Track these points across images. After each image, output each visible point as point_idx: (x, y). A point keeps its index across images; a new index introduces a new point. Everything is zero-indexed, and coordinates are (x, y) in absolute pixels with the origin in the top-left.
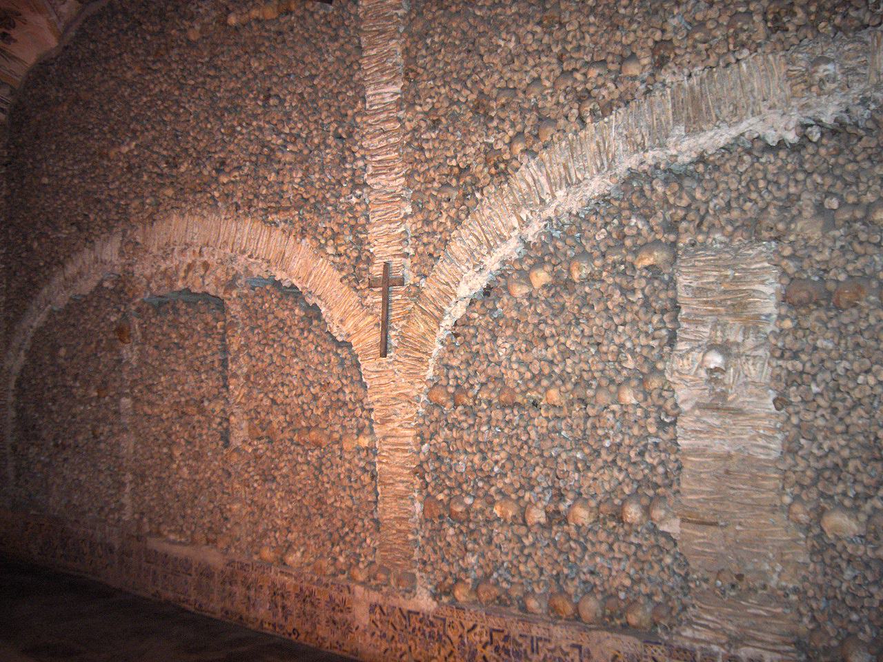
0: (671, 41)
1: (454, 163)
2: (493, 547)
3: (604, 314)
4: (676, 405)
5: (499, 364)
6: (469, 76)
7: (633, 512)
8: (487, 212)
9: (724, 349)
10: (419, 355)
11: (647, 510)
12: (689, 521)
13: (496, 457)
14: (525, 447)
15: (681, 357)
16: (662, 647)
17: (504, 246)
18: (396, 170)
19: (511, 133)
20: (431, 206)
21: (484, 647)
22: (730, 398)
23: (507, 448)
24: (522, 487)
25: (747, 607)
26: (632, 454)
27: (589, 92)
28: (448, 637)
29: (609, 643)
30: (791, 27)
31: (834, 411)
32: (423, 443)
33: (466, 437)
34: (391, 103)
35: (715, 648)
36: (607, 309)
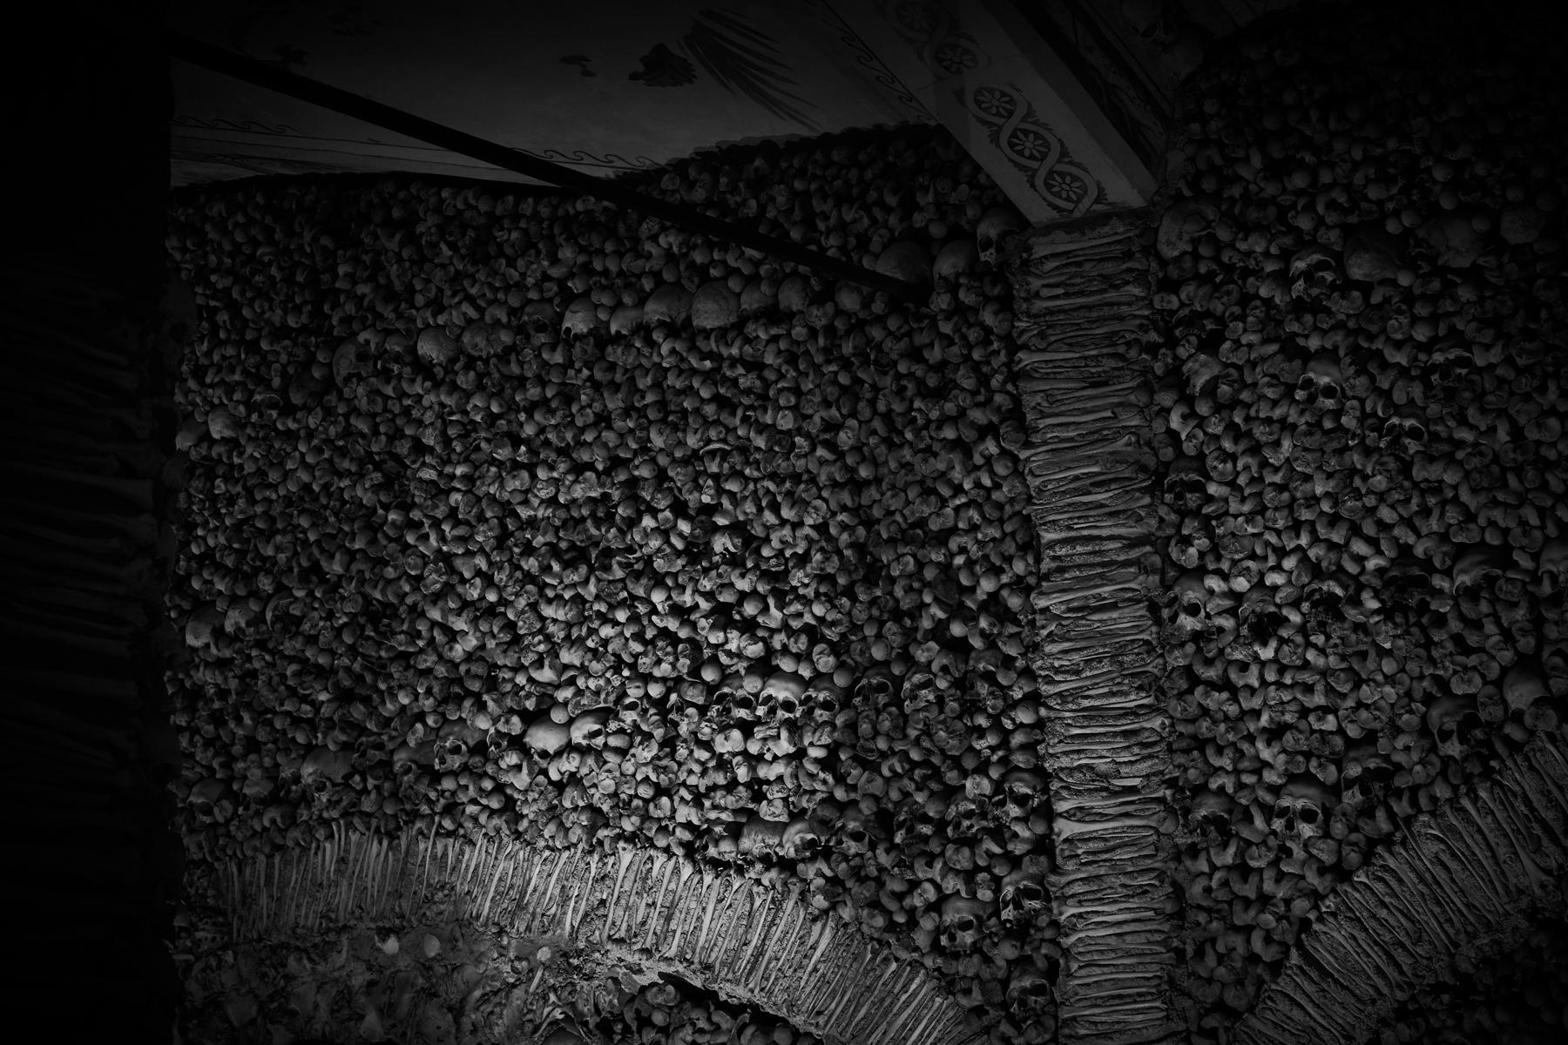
1: (1330, 723)
6: (1371, 511)
19: (1507, 656)
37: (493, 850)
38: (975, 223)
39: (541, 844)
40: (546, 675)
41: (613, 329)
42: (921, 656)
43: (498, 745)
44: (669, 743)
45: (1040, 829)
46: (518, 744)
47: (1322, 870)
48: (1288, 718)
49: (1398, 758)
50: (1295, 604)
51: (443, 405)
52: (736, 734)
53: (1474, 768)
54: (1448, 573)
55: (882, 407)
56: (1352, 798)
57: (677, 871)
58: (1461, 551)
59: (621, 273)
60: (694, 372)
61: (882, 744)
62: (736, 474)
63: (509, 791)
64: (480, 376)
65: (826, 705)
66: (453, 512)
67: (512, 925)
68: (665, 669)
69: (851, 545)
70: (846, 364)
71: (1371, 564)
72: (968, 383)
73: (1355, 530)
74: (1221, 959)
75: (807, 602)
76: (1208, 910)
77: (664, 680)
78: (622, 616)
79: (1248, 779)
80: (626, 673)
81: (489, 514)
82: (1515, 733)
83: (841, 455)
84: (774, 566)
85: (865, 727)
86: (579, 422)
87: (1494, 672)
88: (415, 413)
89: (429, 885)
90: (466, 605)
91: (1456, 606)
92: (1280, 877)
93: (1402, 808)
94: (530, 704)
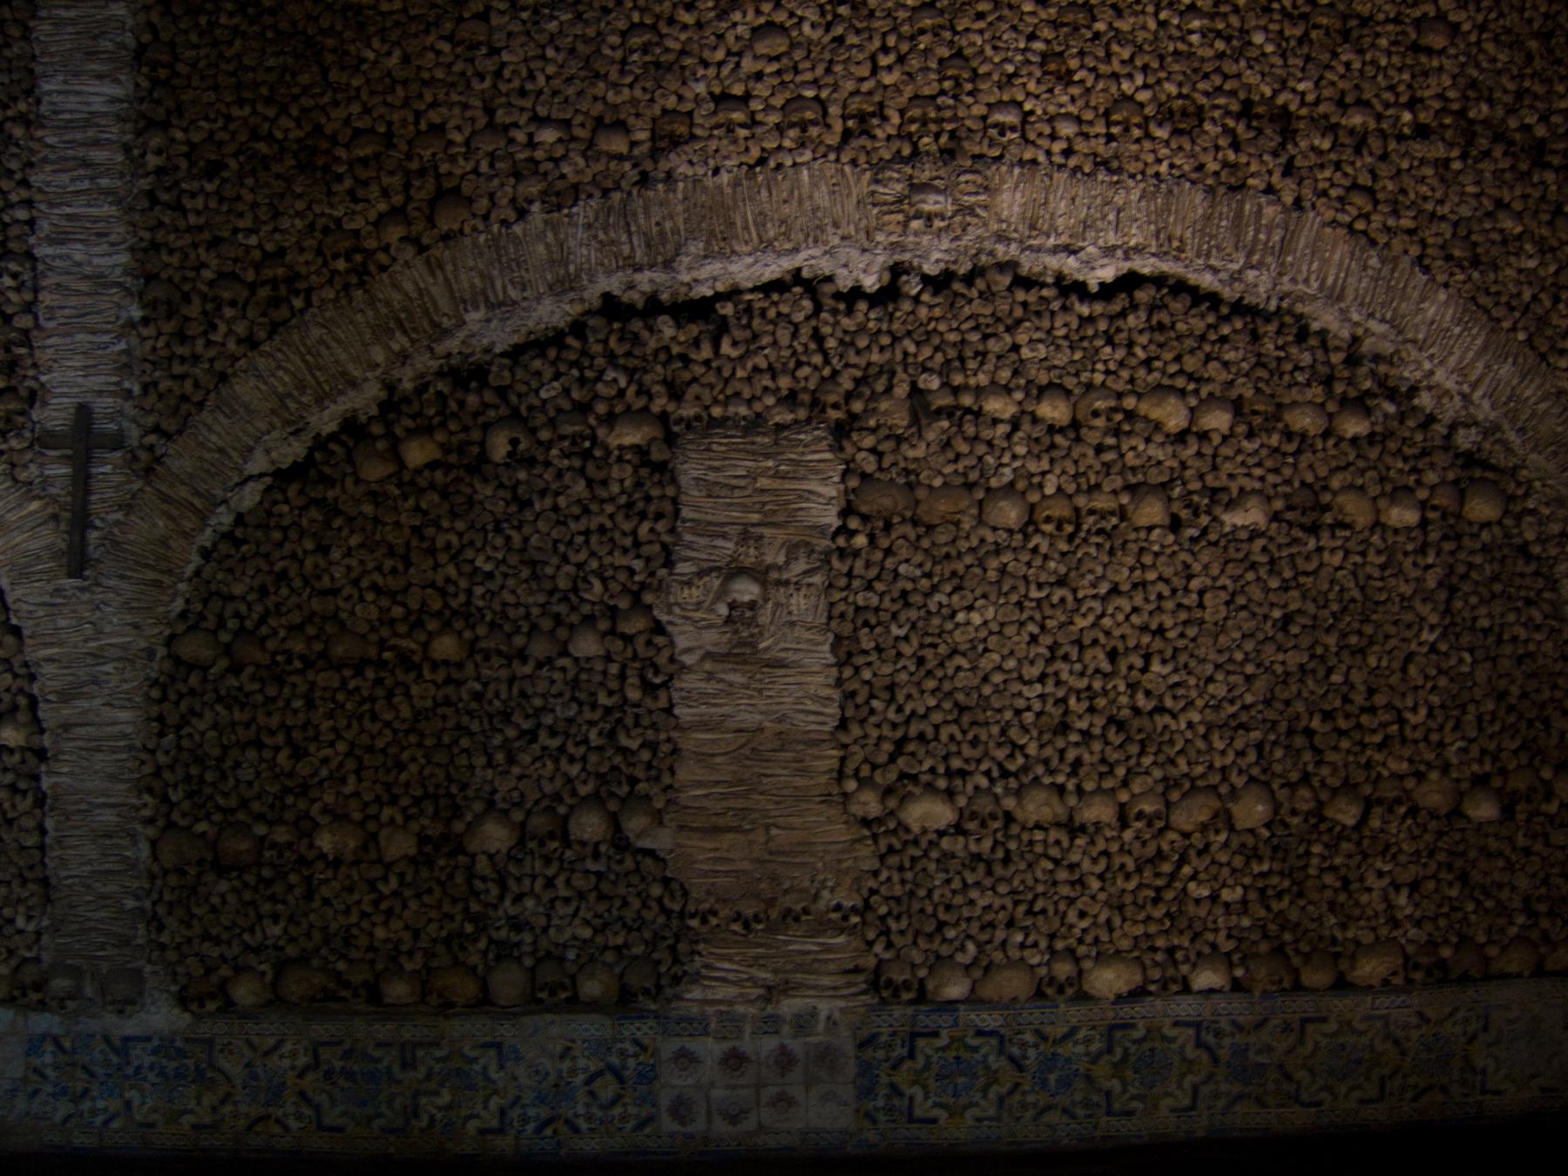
0: (690, 114)
2: (317, 904)
3: (553, 516)
4: (672, 660)
5: (334, 592)
6: (295, 98)
7: (590, 826)
8: (316, 332)
9: (760, 574)
10: (151, 575)
11: (615, 822)
12: (692, 829)
13: (327, 752)
14: (387, 732)
15: (689, 584)
16: (651, 1023)
17: (352, 393)
18: (113, 238)
19: (383, 207)
20: (194, 310)
21: (301, 1075)
22: (763, 645)
23: (349, 735)
24: (378, 799)
25: (787, 943)
26: (593, 735)
27: (537, 163)
28: (220, 1070)
29: (555, 1031)
30: (879, 133)
31: (921, 661)
32: (161, 734)
33: (262, 719)
34: (104, 115)
35: (740, 1009)
36: (555, 508)
45: (28, 297)
47: (240, 341)
48: (226, 234)
49: (303, 271)
50: (235, 155)
53: (355, 280)
54: (347, 146)
56: (264, 293)
58: (358, 133)
71: (292, 135)
73: (284, 110)
74: (160, 396)
76: (154, 363)
79: (191, 274)
82: (382, 258)
87: (372, 216)
91: (351, 168)
92: (209, 343)
93: (298, 303)
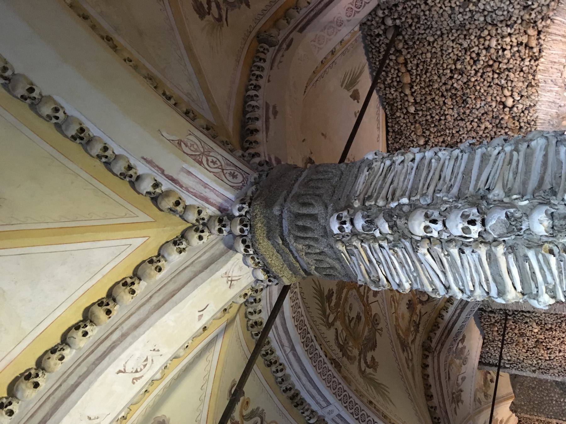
37: (539, 111)
38: (380, 17)
39: (537, 99)
40: (494, 104)
41: (413, 101)
42: (482, 7)
43: (512, 113)
44: (509, 70)
46: (511, 108)
51: (434, 138)
52: (506, 52)
55: (423, 32)
57: (542, 63)
59: (401, 101)
60: (420, 80)
61: (505, 13)
62: (442, 66)
63: (524, 109)
64: (427, 130)
65: (497, 30)
66: (457, 132)
67: (558, 103)
68: (490, 74)
69: (457, 32)
70: (414, 43)
72: (415, 10)
75: (471, 40)
77: (493, 74)
78: (478, 88)
80: (492, 84)
81: (457, 124)
83: (436, 40)
84: (463, 52)
85: (502, 18)
86: (434, 105)
88: (436, 143)
89: (549, 126)
90: (479, 126)
94: (501, 106)
